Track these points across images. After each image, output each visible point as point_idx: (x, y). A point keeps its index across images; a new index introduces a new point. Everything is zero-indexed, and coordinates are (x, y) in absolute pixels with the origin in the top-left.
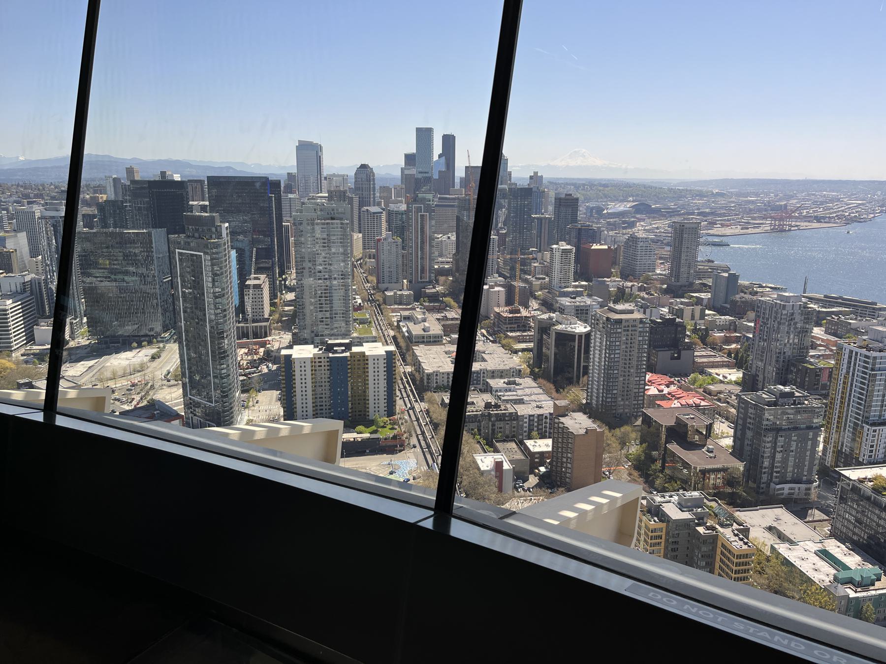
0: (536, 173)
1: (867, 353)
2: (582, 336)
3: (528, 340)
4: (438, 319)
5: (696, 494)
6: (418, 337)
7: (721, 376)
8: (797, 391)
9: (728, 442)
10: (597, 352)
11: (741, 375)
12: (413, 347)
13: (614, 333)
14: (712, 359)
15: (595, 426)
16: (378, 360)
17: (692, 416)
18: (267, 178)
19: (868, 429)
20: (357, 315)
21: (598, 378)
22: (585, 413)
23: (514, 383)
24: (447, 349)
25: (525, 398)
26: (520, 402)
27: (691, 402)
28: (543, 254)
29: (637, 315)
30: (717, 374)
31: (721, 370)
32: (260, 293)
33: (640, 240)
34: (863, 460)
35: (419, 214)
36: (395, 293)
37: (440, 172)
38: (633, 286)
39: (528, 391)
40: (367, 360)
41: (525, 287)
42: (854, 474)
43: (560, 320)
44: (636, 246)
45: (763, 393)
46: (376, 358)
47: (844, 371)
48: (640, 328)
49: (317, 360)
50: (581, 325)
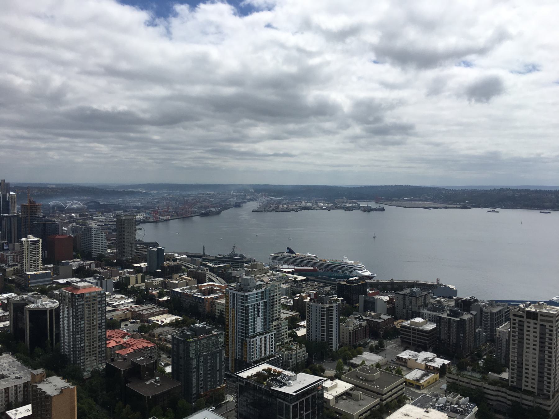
1: (242, 294)
2: (52, 310)
7: (160, 321)
8: (207, 325)
9: (169, 369)
10: (66, 322)
13: (77, 306)
14: (152, 311)
15: (68, 384)
17: (143, 358)
19: (249, 341)
22: (58, 376)
27: (140, 347)
28: (14, 245)
30: (157, 321)
33: (94, 229)
34: (249, 361)
38: (91, 264)
42: (244, 374)
43: (32, 299)
44: (90, 234)
45: (188, 331)
47: (232, 307)
48: (98, 298)
50: (51, 302)
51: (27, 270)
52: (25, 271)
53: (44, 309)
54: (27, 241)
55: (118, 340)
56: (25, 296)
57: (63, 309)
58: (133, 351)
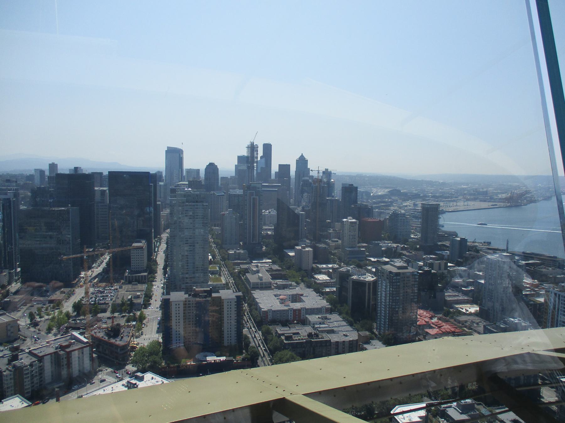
0: (327, 170)
2: (370, 283)
3: (330, 286)
4: (267, 271)
5: (469, 401)
6: (254, 283)
7: (464, 309)
8: (523, 322)
11: (478, 309)
12: (252, 292)
14: (456, 298)
16: (231, 302)
18: (148, 173)
20: (211, 268)
21: (385, 314)
22: (380, 341)
23: (326, 318)
24: (275, 293)
25: (335, 329)
26: (332, 332)
29: (410, 270)
31: (463, 306)
32: (142, 252)
33: (399, 215)
35: (252, 197)
36: (235, 252)
37: (262, 168)
38: (398, 246)
39: (336, 324)
40: (223, 303)
41: (325, 247)
44: (397, 220)
46: (230, 301)
49: (187, 303)
50: (369, 276)
51: (346, 247)
52: (345, 247)
53: (364, 282)
54: (347, 222)
55: (427, 320)
56: (349, 268)
57: (382, 284)
58: (442, 333)
